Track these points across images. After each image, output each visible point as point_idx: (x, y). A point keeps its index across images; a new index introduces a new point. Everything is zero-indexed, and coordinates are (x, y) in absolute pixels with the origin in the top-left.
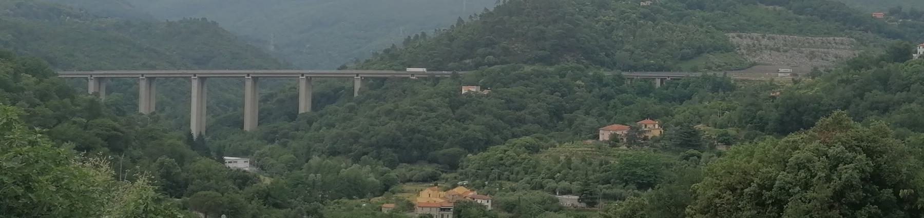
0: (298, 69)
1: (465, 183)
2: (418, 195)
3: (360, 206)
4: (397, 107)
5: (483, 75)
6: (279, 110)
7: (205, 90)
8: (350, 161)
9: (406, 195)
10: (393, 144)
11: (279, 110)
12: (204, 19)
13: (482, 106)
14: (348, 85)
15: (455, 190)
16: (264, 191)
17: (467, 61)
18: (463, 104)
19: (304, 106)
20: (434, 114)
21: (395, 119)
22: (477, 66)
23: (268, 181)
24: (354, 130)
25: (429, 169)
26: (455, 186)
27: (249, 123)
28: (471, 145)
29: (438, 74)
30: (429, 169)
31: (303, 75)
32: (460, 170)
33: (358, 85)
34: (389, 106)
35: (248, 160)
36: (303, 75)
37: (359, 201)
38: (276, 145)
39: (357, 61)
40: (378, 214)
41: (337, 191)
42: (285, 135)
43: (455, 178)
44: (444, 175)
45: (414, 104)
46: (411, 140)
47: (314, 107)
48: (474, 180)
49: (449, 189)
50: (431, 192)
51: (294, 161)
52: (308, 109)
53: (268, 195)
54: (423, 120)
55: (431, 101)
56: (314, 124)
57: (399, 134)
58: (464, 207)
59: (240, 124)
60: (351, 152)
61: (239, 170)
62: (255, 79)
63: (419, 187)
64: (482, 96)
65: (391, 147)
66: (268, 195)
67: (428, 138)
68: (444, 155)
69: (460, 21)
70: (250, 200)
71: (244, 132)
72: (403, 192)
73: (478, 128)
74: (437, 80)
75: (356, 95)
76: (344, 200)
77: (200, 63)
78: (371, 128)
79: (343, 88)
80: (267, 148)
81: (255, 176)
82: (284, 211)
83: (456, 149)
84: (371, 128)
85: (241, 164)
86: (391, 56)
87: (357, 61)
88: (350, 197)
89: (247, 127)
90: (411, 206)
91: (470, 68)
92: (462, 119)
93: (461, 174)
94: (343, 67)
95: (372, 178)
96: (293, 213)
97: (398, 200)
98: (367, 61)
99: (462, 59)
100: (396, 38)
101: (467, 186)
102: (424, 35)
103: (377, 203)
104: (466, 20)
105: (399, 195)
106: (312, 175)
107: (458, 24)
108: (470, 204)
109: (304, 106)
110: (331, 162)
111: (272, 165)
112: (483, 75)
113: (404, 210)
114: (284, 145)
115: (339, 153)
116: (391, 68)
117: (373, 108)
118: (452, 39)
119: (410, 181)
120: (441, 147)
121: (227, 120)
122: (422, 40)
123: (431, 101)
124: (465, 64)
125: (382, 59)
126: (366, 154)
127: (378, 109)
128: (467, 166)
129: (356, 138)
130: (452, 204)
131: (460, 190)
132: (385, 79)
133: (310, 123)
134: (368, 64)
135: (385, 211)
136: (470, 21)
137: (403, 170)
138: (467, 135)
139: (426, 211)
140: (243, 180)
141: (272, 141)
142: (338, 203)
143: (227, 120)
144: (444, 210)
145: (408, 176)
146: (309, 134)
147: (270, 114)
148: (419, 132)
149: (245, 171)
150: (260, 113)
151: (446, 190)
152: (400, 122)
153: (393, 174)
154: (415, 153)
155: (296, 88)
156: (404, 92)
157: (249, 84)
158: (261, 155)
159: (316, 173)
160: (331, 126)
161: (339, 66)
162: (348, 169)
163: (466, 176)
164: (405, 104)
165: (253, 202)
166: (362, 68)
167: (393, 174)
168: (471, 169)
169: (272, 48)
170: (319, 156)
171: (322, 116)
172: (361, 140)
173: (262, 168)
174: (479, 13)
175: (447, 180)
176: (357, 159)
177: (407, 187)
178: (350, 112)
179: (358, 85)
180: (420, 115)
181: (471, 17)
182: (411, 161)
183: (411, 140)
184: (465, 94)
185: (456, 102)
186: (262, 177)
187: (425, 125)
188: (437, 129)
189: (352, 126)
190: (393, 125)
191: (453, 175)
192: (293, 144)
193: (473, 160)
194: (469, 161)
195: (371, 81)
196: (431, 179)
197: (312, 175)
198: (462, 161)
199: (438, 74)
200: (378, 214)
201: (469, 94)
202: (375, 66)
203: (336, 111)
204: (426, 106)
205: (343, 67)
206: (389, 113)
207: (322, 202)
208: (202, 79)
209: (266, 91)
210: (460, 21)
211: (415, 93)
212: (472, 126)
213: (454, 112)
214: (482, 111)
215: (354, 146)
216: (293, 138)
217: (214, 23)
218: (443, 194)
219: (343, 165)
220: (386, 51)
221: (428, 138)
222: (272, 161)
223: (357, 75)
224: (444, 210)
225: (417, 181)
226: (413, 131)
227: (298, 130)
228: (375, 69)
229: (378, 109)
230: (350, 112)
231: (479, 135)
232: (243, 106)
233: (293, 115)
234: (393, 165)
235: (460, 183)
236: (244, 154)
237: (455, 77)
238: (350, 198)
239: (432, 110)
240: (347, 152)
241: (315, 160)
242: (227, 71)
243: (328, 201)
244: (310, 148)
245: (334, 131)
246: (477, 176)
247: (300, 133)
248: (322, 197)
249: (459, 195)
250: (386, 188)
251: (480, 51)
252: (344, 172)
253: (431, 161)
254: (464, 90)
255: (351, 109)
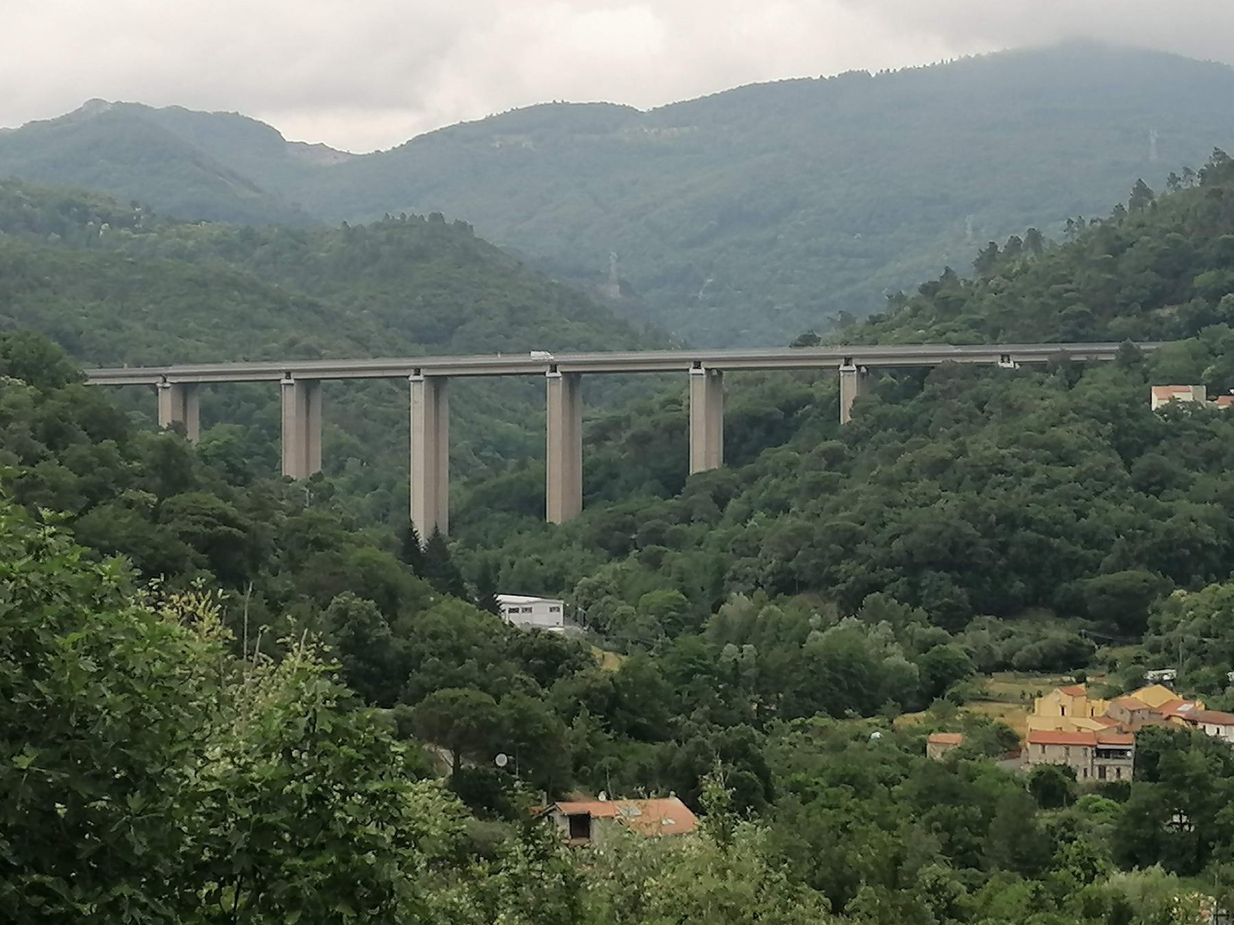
0: (686, 347)
1: (1169, 674)
2: (1031, 709)
3: (867, 739)
4: (963, 452)
5: (1212, 352)
6: (637, 462)
7: (445, 423)
8: (832, 607)
9: (993, 708)
10: (953, 558)
11: (637, 462)
12: (437, 217)
13: (1213, 444)
14: (821, 390)
15: (1139, 695)
16: (604, 690)
17: (1165, 312)
18: (1156, 440)
19: (704, 452)
20: (1070, 472)
21: (958, 486)
22: (1196, 325)
23: (612, 663)
24: (843, 519)
25: (1059, 633)
26: (1137, 683)
27: (560, 504)
28: (1182, 563)
29: (1078, 351)
30: (1059, 633)
31: (697, 365)
32: (1150, 638)
33: (850, 390)
34: (940, 449)
35: (560, 604)
36: (697, 365)
37: (861, 723)
38: (631, 562)
39: (847, 319)
40: (917, 761)
41: (798, 694)
42: (655, 536)
43: (1138, 660)
44: (1102, 652)
45: (1012, 443)
46: (1003, 548)
47: (731, 457)
48: (1194, 667)
49: (1120, 693)
50: (1067, 700)
51: (681, 608)
52: (716, 463)
53: (615, 701)
54: (1039, 488)
55: (1060, 432)
56: (732, 502)
57: (969, 529)
58: (1167, 745)
59: (537, 505)
60: (835, 582)
61: (536, 631)
62: (572, 379)
63: (1031, 685)
64: (1216, 414)
65: (947, 566)
66: (615, 701)
67: (1055, 542)
68: (1102, 591)
69: (1142, 191)
70: (569, 715)
71: (548, 528)
72: (985, 698)
73: (1199, 510)
74: (1075, 372)
75: (845, 418)
76: (821, 720)
77: (432, 337)
78: (889, 514)
79: (809, 399)
80: (606, 572)
81: (578, 647)
82: (657, 748)
83: (1138, 575)
84: (889, 514)
85: (541, 615)
86: (941, 303)
87: (847, 319)
88: (837, 713)
89: (555, 514)
90: (1009, 742)
91: (1177, 334)
92: (1155, 484)
93: (1154, 649)
94: (808, 340)
95: (897, 658)
96: (681, 754)
97: (971, 724)
98: (874, 320)
99: (1148, 305)
100: (953, 250)
101: (1174, 685)
102: (1035, 237)
103: (915, 732)
104: (1160, 189)
105: (976, 708)
106: (730, 649)
107: (1135, 203)
108: (1184, 739)
109: (704, 452)
110: (783, 611)
111: (623, 617)
112: (1212, 352)
113: (991, 752)
114: (654, 563)
115: (803, 586)
116: (941, 337)
117: (893, 456)
118: (1117, 247)
119: (1004, 666)
120: (1094, 569)
121: (502, 495)
122: (1030, 255)
123: (1060, 432)
124: (1160, 321)
125: (916, 311)
126: (877, 587)
127: (907, 457)
128: (1172, 627)
129: (849, 542)
130: (1130, 738)
131: (1152, 697)
132: (927, 369)
133: (721, 500)
134: (877, 329)
135: (936, 754)
136: (1170, 192)
137: (983, 633)
138: (1169, 532)
139: (1055, 756)
140: (547, 658)
141: (621, 552)
142: (802, 726)
143: (502, 495)
144: (1107, 753)
145: (999, 650)
146: (719, 532)
147: (615, 476)
148: (1028, 523)
149: (551, 636)
150: (587, 471)
151: (1111, 694)
152: (972, 495)
153: (956, 647)
154: (1019, 586)
155: (677, 403)
156: (980, 407)
157: (556, 392)
158: (592, 590)
159: (741, 641)
160: (779, 507)
161: (795, 336)
162: (831, 631)
163: (1172, 658)
164: (985, 443)
165: (576, 721)
166: (860, 341)
167: (956, 647)
168: (1186, 632)
169: (614, 291)
170: (750, 594)
171: (751, 479)
172: (862, 548)
173: (597, 626)
174: (1199, 166)
175: (1112, 666)
176: (851, 604)
177: (997, 684)
178: (829, 467)
179: (850, 390)
180: (1028, 473)
181: (1173, 179)
182: (1006, 609)
183: (1003, 548)
184: (1160, 411)
185: (1132, 434)
186: (597, 652)
187: (1044, 504)
188: (1080, 514)
189: (835, 510)
190: (950, 504)
191: (1131, 651)
192: (677, 559)
193: (1190, 606)
194: (1176, 609)
195: (887, 378)
196: (1066, 663)
197: (730, 649)
198: (1156, 611)
199: (1078, 351)
200: (917, 761)
201: (1172, 411)
202: (896, 333)
203: (790, 465)
204: (1045, 446)
205: (808, 340)
206: (938, 468)
207: (758, 726)
208: (437, 383)
209: (601, 413)
210: (1142, 191)
211: (1012, 410)
212: (1184, 506)
213: (1128, 465)
214: (1213, 460)
215: (843, 567)
216: (677, 543)
217: (463, 227)
218: (1102, 706)
219: (815, 619)
220: (928, 290)
221: (1055, 542)
222: (623, 608)
223: (848, 361)
224: (1107, 753)
225: (1026, 668)
226: (1010, 520)
227: (688, 521)
228: (897, 342)
229: (907, 457)
230: (829, 467)
231: (1206, 532)
232: (541, 453)
233: (674, 479)
234: (954, 620)
235: (1151, 675)
236: (549, 587)
237: (1129, 360)
238: (838, 714)
239: (1065, 459)
240: (822, 582)
241: (738, 604)
242: (499, 359)
243: (776, 721)
244: (721, 571)
245: (787, 523)
246: (1202, 655)
247: (695, 530)
248: (760, 710)
249: (1151, 711)
250: (936, 686)
251: (1204, 278)
252: (817, 640)
253: (1065, 611)
254: (1158, 400)
255: (833, 459)
